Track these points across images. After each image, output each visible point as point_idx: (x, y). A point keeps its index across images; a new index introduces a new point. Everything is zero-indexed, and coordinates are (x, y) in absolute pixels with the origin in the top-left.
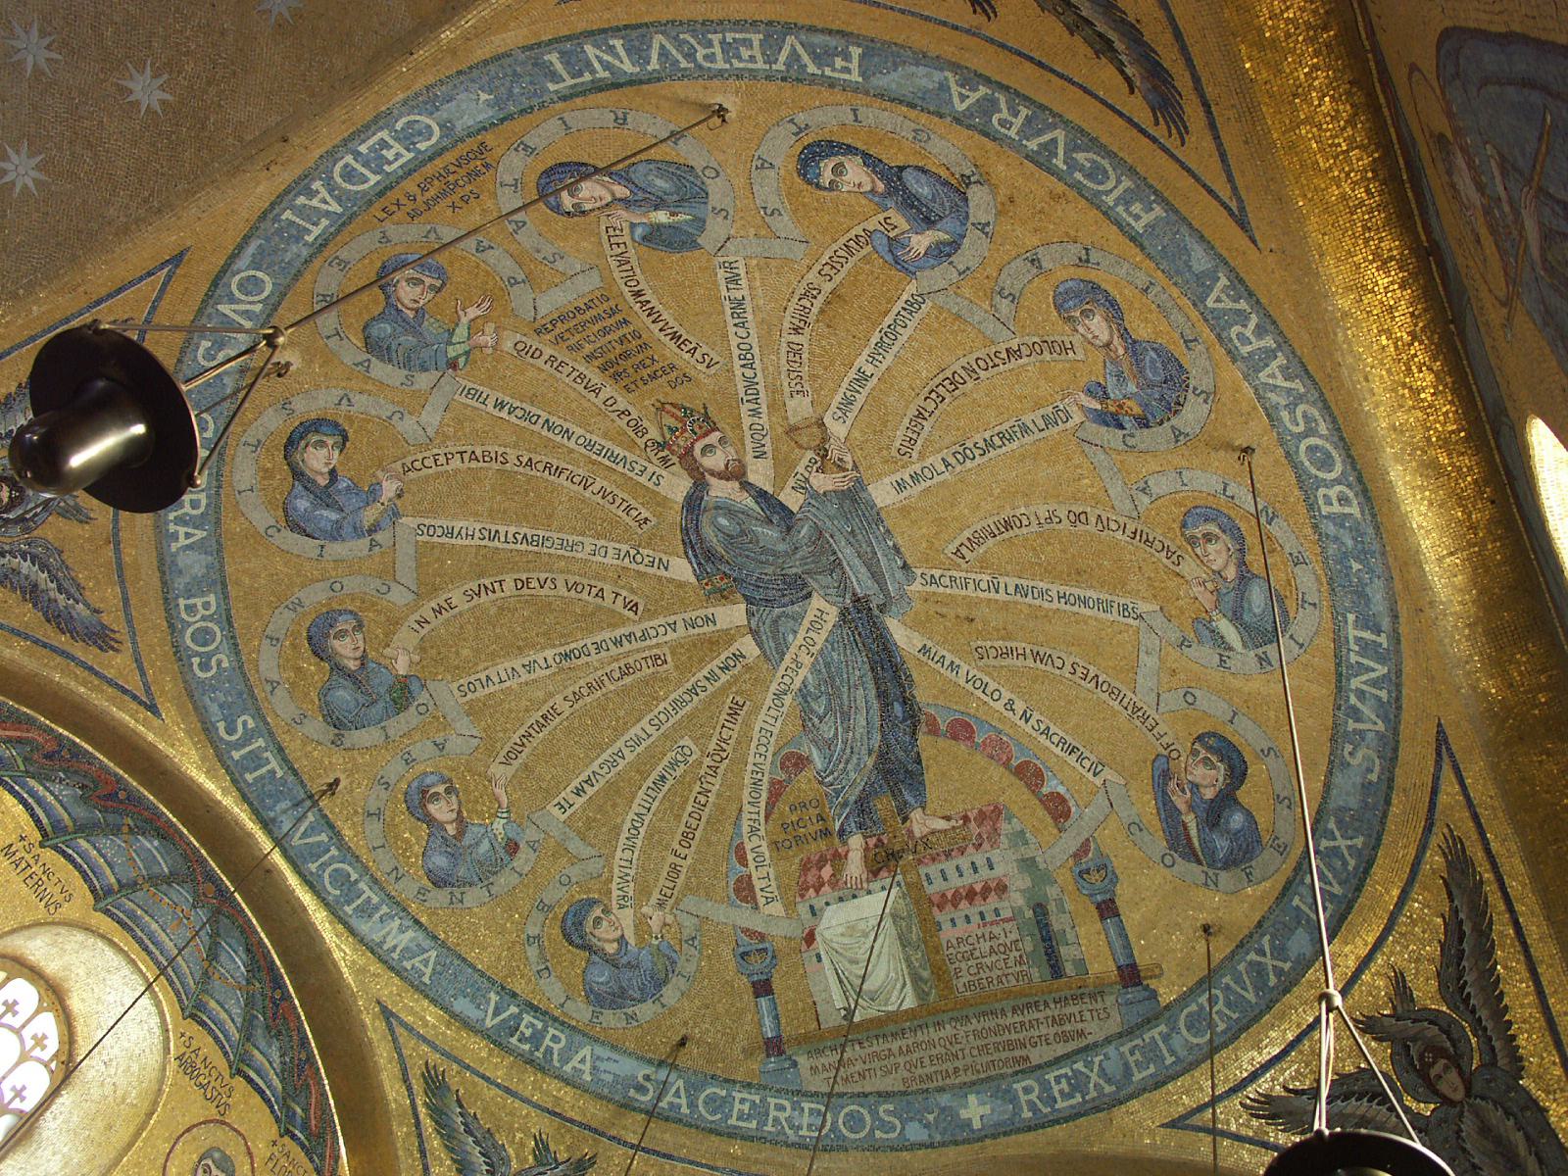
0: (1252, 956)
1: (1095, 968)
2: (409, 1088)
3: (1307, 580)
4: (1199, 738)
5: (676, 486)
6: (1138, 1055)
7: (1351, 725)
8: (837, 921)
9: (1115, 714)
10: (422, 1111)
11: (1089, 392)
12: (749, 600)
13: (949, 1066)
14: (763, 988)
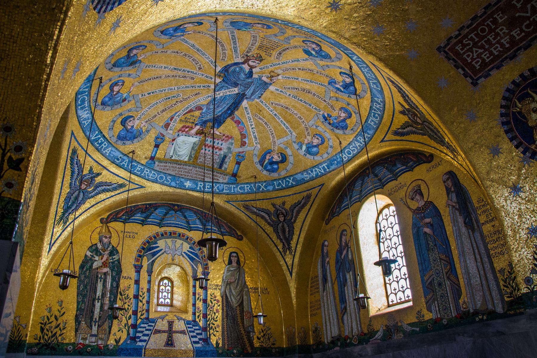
0: (260, 185)
1: (228, 171)
2: (68, 152)
3: (325, 156)
4: (281, 153)
5: (240, 60)
8: (182, 139)
9: (270, 139)
10: (69, 158)
11: (328, 115)
12: (223, 80)
13: (187, 174)
14: (157, 146)
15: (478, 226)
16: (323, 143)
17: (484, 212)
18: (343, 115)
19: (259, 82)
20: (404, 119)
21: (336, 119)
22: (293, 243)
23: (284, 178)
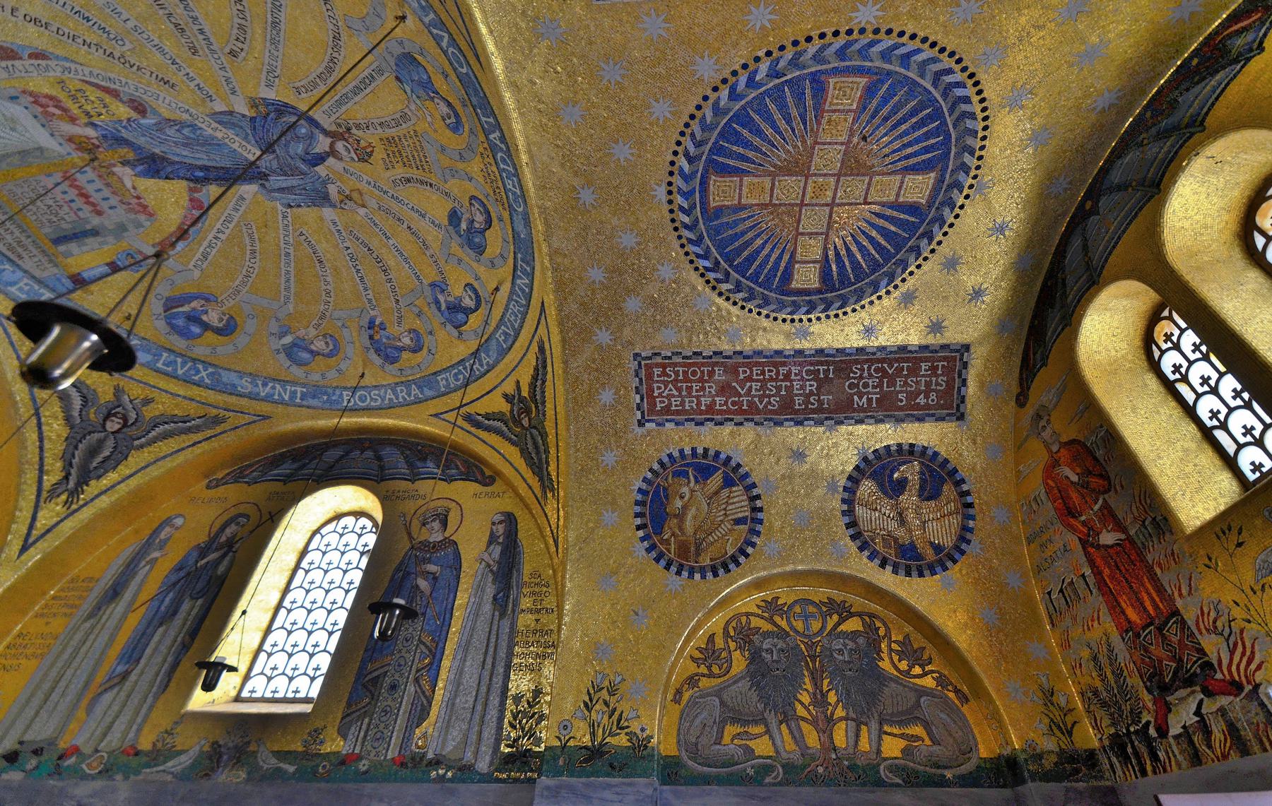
3: (315, 377)
5: (326, 123)
6: (27, 288)
7: (260, 383)
11: (382, 323)
12: (253, 119)
15: (513, 611)
16: (330, 355)
17: (534, 593)
18: (407, 341)
19: (318, 185)
20: (505, 407)
21: (388, 338)
22: (93, 487)
23: (194, 360)
